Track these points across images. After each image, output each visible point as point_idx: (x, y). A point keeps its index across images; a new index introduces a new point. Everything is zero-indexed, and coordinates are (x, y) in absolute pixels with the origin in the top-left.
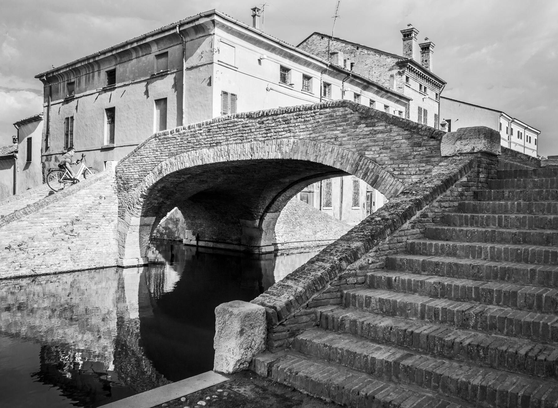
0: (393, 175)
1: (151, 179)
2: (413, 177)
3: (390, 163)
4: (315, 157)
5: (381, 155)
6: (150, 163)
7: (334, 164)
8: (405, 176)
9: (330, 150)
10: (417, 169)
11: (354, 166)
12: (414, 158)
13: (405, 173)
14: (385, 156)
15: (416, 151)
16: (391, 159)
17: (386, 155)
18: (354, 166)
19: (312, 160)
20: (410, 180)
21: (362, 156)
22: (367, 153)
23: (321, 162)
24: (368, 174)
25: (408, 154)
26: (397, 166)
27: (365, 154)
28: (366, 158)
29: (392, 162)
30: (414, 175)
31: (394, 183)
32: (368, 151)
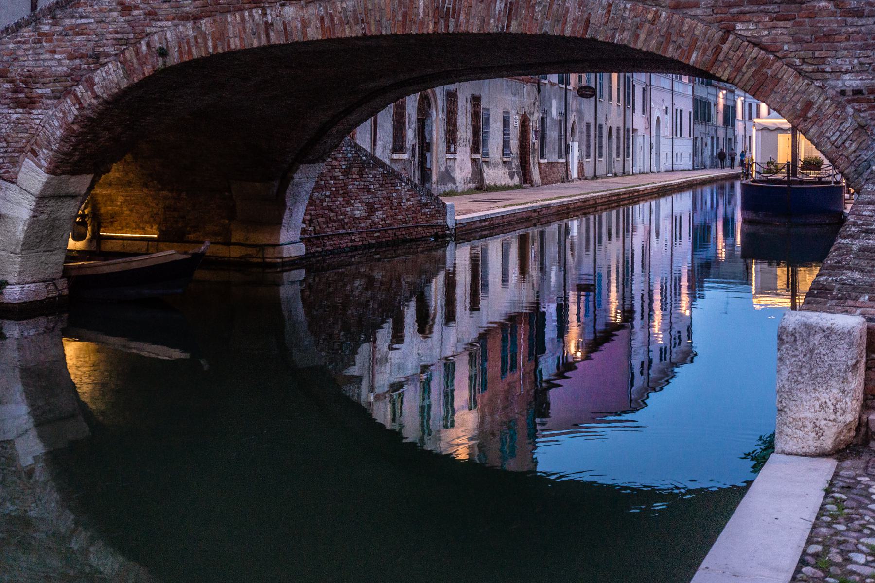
0: (800, 73)
1: (110, 77)
2: (847, 77)
3: (793, 47)
4: (610, 33)
5: (774, 31)
6: (110, 36)
7: (658, 48)
8: (828, 75)
9: (650, 16)
10: (856, 61)
11: (709, 53)
12: (847, 40)
13: (828, 69)
14: (782, 34)
15: (852, 25)
16: (797, 41)
17: (784, 31)
18: (709, 53)
19: (601, 38)
20: (840, 83)
21: (729, 31)
22: (739, 26)
23: (625, 42)
24: (744, 69)
25: (834, 30)
26: (809, 54)
27: (734, 29)
28: (739, 36)
29: (798, 46)
30: (847, 72)
31: (803, 89)
32: (743, 22)
